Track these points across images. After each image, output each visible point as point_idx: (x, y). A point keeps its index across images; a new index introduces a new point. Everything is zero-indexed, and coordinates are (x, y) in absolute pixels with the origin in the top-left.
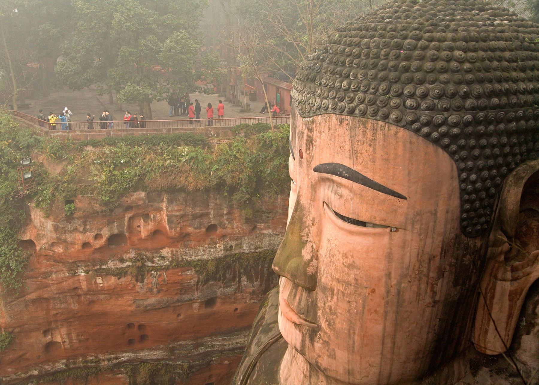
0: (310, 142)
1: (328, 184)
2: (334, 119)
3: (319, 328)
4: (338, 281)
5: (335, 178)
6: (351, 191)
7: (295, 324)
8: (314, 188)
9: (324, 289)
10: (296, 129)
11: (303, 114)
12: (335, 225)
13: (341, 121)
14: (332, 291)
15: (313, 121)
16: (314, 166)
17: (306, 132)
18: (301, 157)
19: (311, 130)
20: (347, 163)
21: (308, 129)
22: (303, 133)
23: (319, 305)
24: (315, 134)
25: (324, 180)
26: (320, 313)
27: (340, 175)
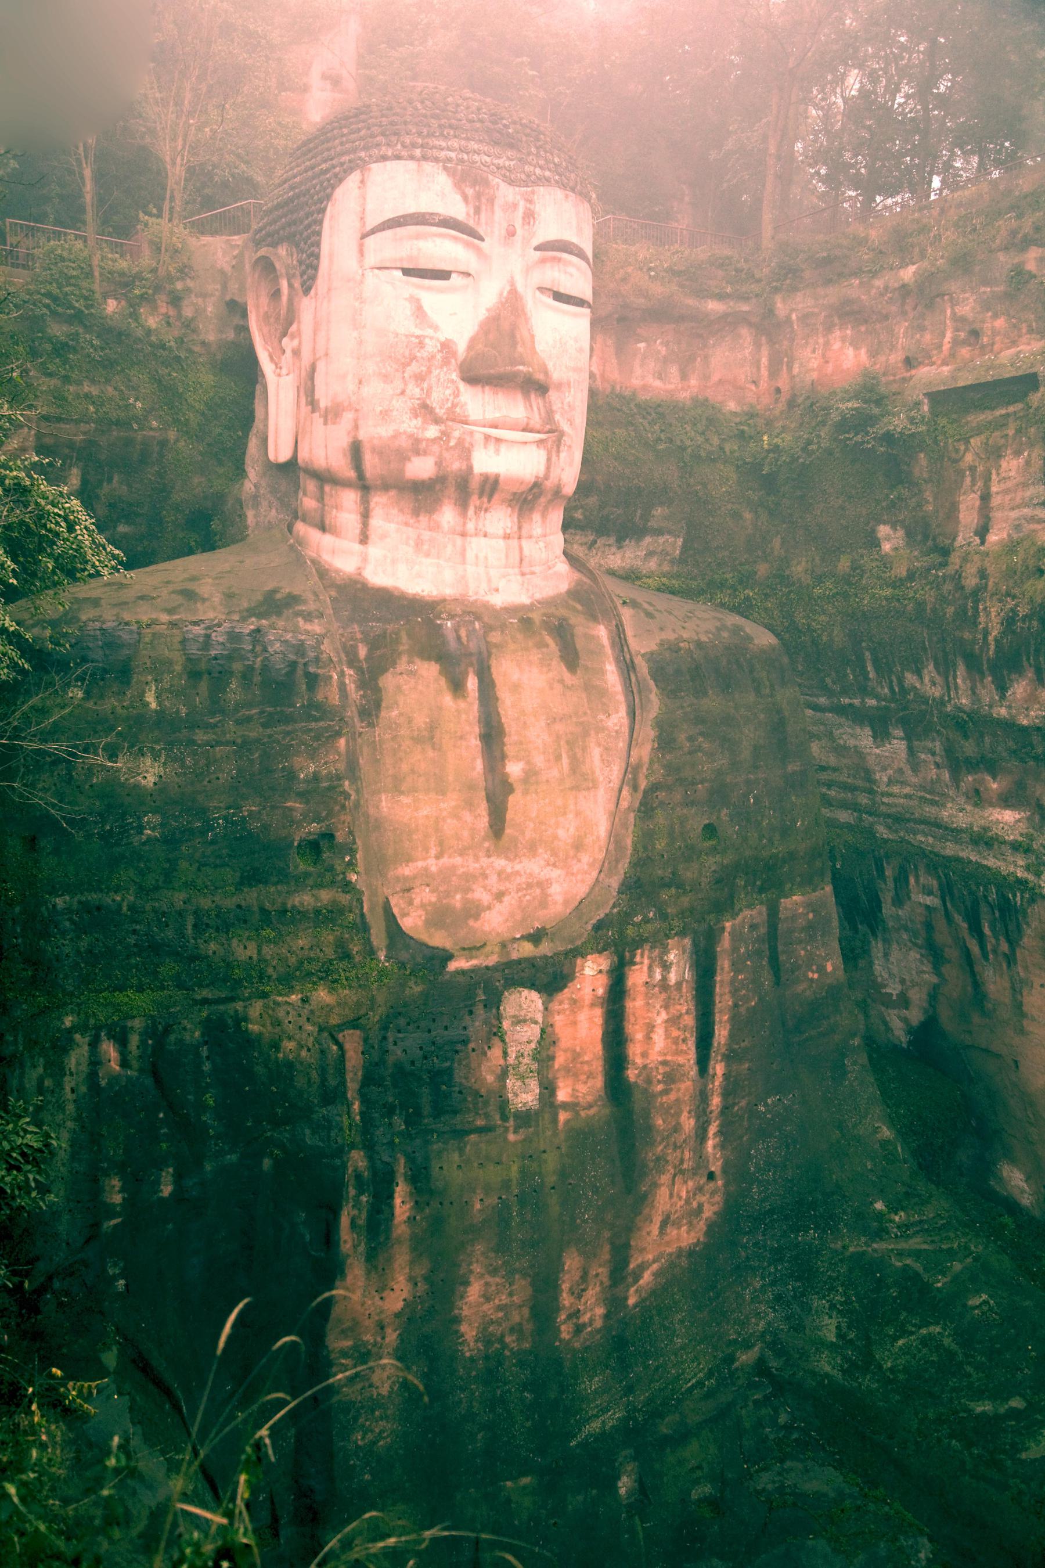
0: (529, 216)
1: (548, 265)
2: (559, 193)
3: (562, 434)
4: (576, 370)
5: (565, 256)
6: (579, 269)
7: (540, 443)
8: (528, 270)
9: (559, 386)
10: (491, 201)
11: (511, 182)
12: (556, 310)
13: (567, 196)
14: (569, 384)
15: (533, 192)
16: (535, 242)
17: (522, 203)
18: (511, 233)
19: (531, 202)
20: (574, 240)
21: (527, 200)
22: (515, 206)
23: (554, 408)
24: (537, 208)
25: (543, 261)
26: (557, 417)
27: (571, 253)
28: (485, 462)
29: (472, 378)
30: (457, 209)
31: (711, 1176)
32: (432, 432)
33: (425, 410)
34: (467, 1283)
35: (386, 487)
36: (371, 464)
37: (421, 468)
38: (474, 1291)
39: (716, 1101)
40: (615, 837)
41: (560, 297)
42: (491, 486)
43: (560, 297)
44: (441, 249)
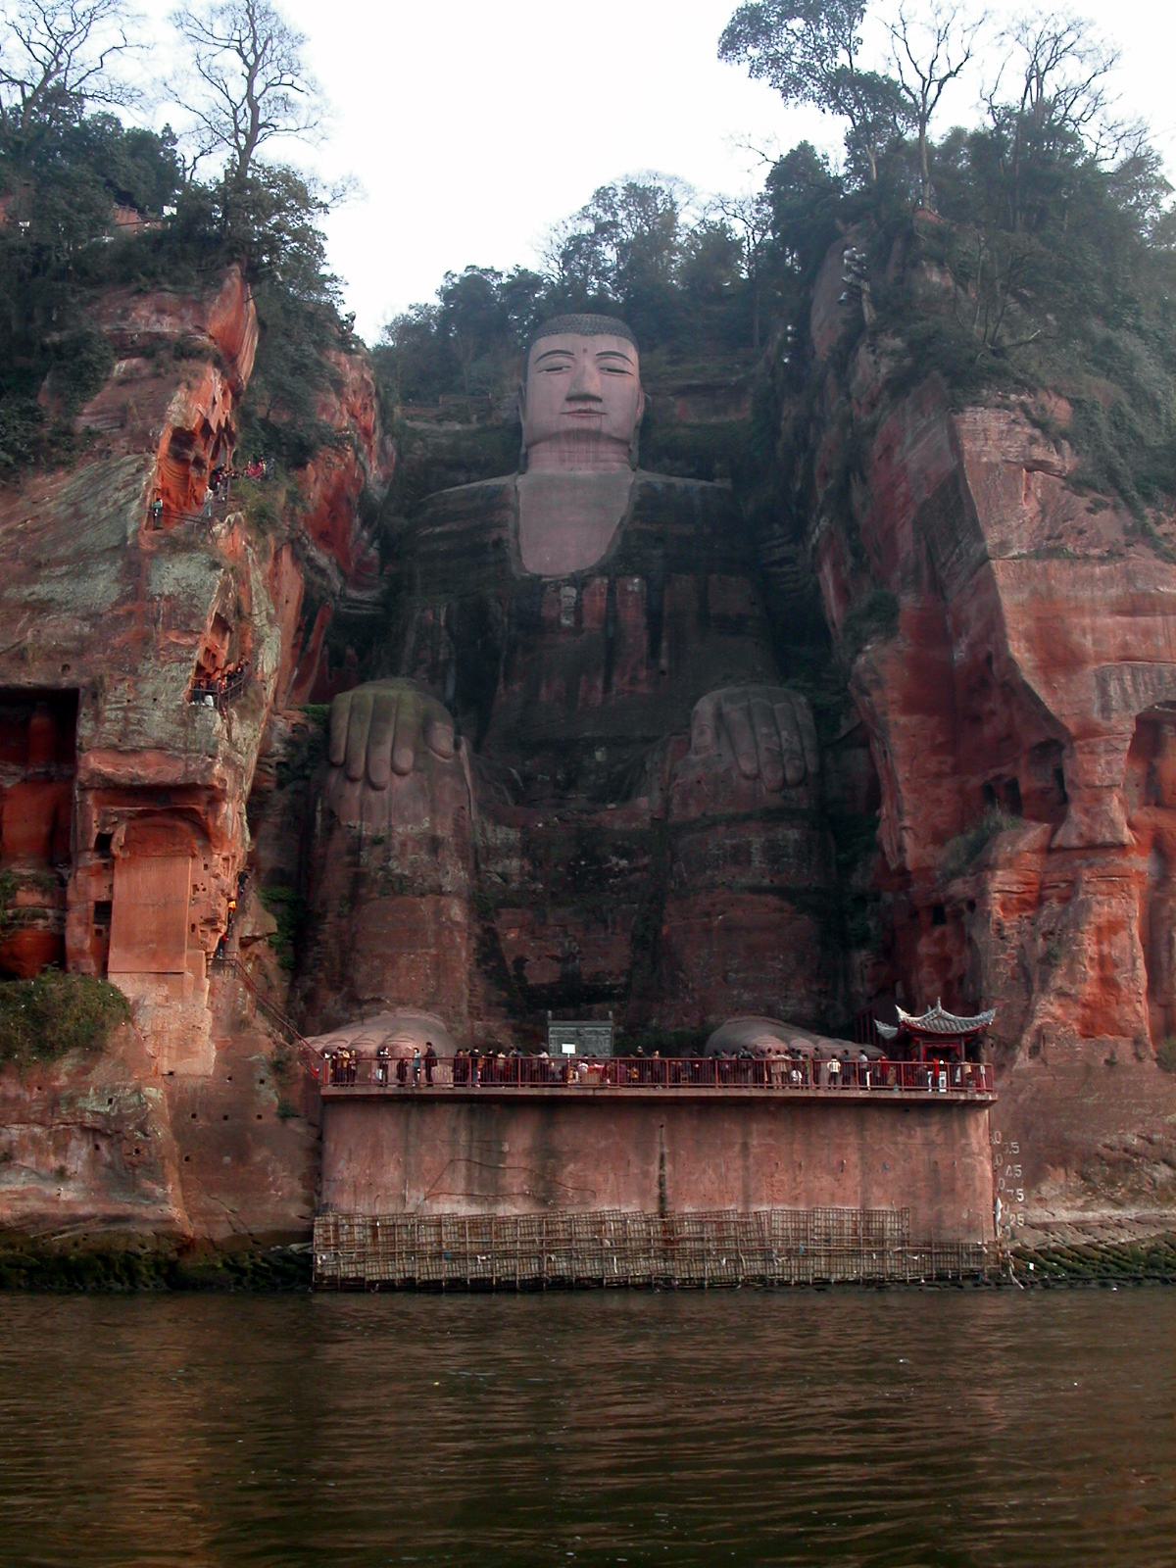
29: (570, 399)
44: (562, 360)
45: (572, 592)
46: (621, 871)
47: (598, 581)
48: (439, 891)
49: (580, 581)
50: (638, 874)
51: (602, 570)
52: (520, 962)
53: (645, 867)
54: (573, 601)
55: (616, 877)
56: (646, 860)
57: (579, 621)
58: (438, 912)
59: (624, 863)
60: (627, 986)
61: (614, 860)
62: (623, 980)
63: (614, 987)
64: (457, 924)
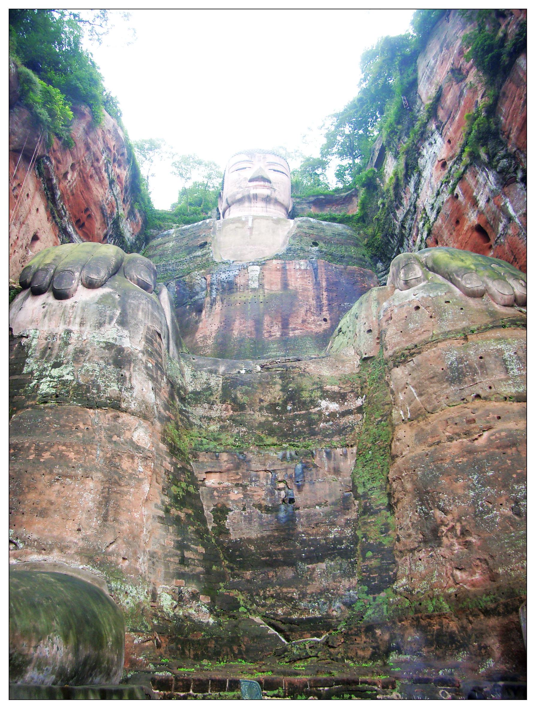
28: (253, 192)
29: (251, 181)
30: (247, 158)
31: (325, 320)
32: (241, 190)
33: (240, 187)
34: (235, 321)
35: (233, 203)
36: (229, 202)
37: (239, 196)
38: (237, 323)
39: (325, 302)
40: (284, 243)
41: (274, 170)
42: (256, 197)
43: (274, 170)
45: (258, 268)
46: (333, 415)
47: (275, 262)
48: (115, 405)
49: (262, 264)
50: (351, 417)
51: (277, 257)
52: (221, 512)
53: (360, 410)
54: (258, 273)
55: (327, 421)
56: (359, 402)
57: (261, 285)
58: (114, 431)
59: (334, 407)
60: (355, 540)
61: (324, 403)
62: (348, 532)
63: (338, 540)
64: (138, 448)
